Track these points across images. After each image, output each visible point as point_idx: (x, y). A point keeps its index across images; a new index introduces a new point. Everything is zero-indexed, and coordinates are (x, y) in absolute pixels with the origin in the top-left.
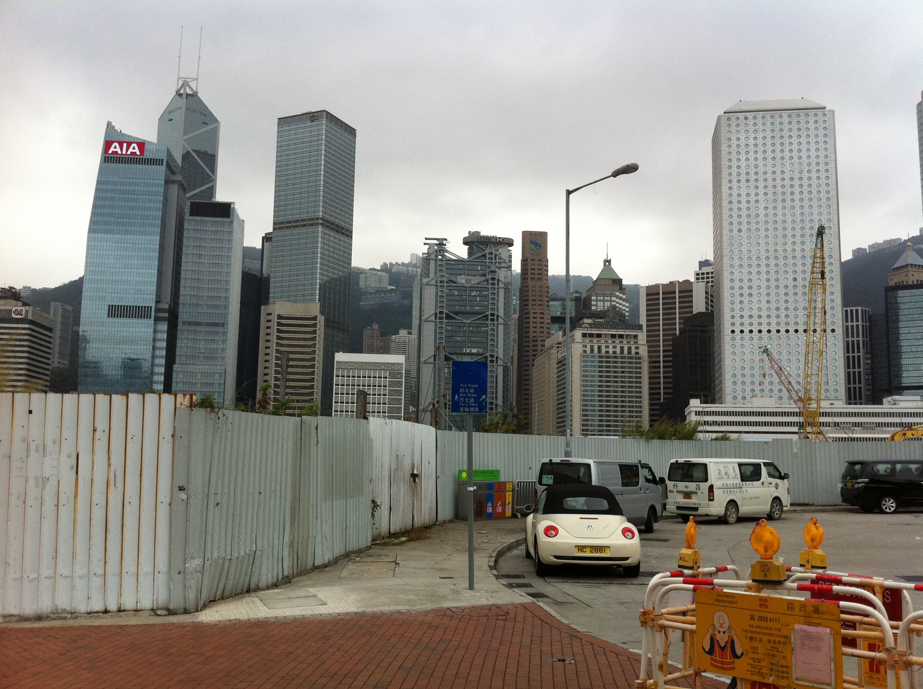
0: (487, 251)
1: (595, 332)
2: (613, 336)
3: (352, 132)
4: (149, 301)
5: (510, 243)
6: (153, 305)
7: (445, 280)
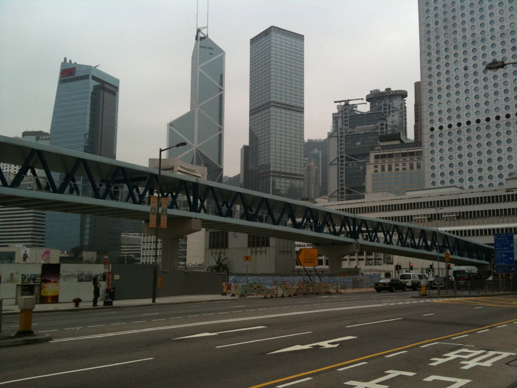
0: (383, 103)
1: (386, 153)
2: (404, 155)
5: (403, 95)
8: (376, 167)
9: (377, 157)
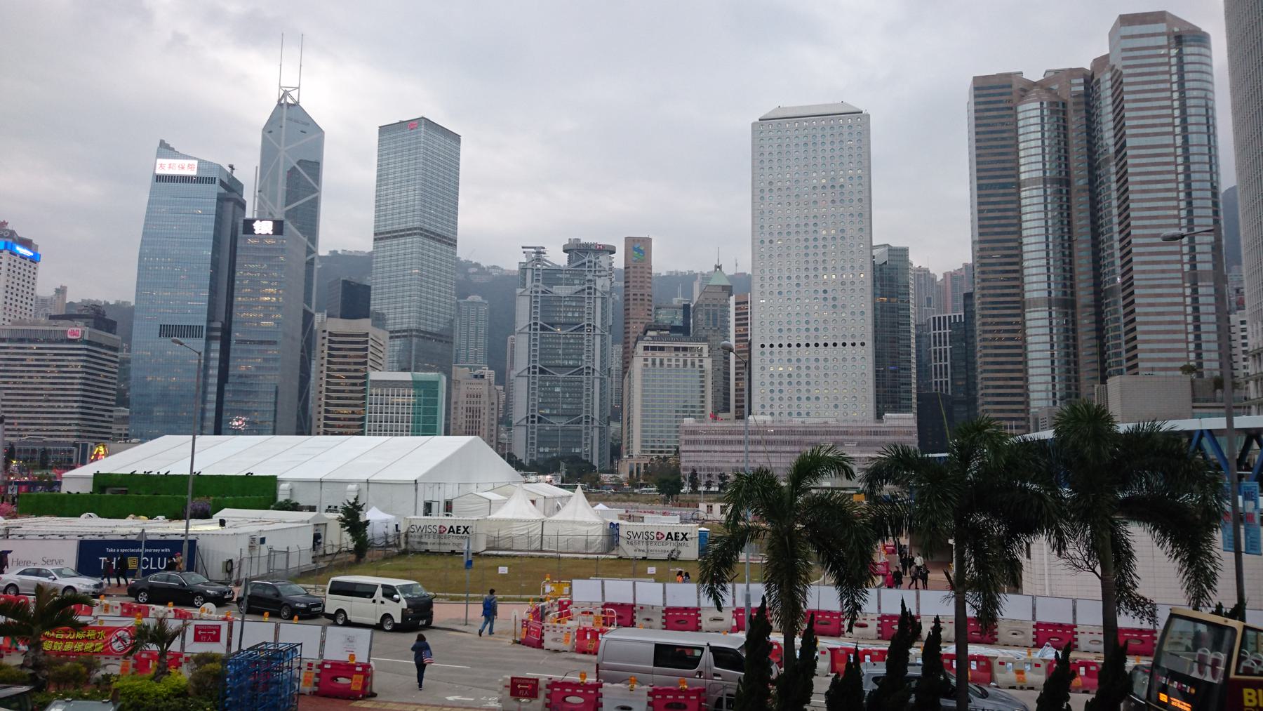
0: (586, 259)
2: (677, 349)
3: (456, 138)
4: (202, 321)
6: (205, 324)
7: (540, 290)
8: (646, 360)
9: (646, 348)
